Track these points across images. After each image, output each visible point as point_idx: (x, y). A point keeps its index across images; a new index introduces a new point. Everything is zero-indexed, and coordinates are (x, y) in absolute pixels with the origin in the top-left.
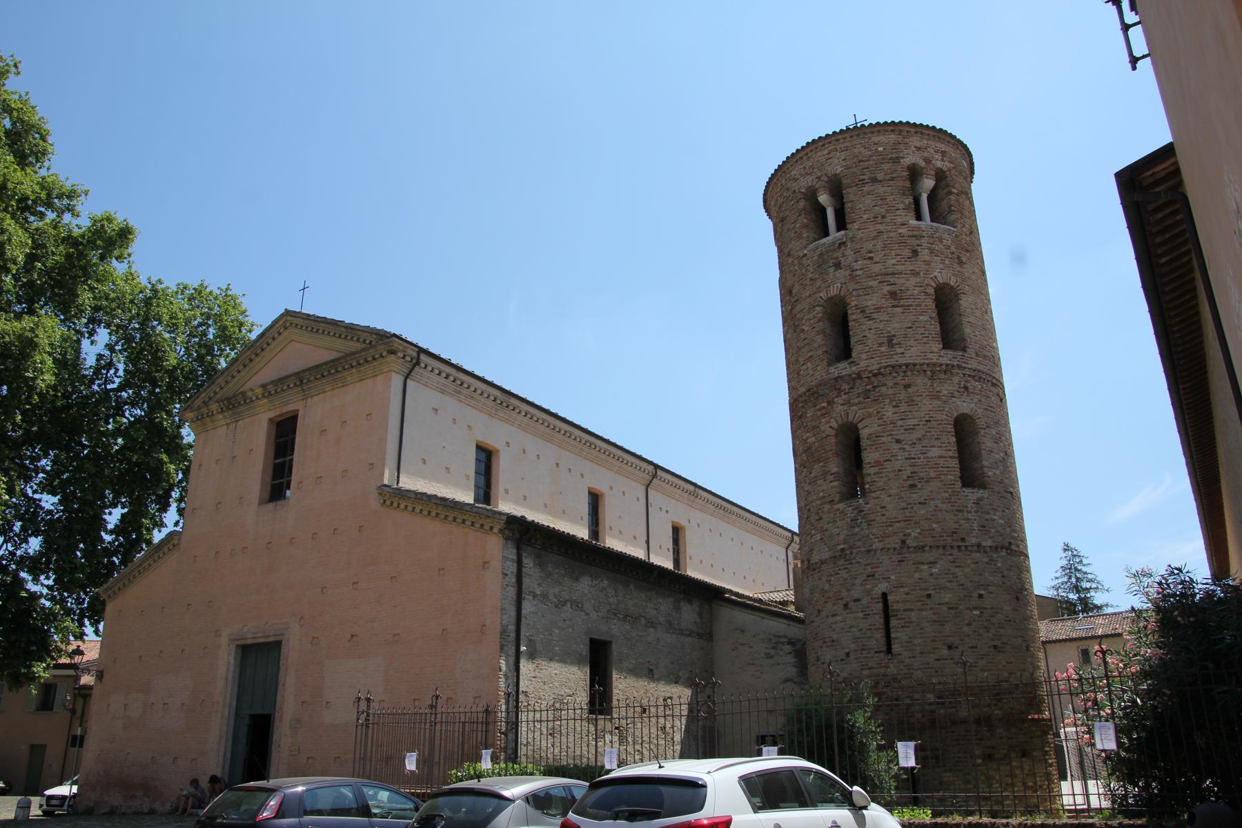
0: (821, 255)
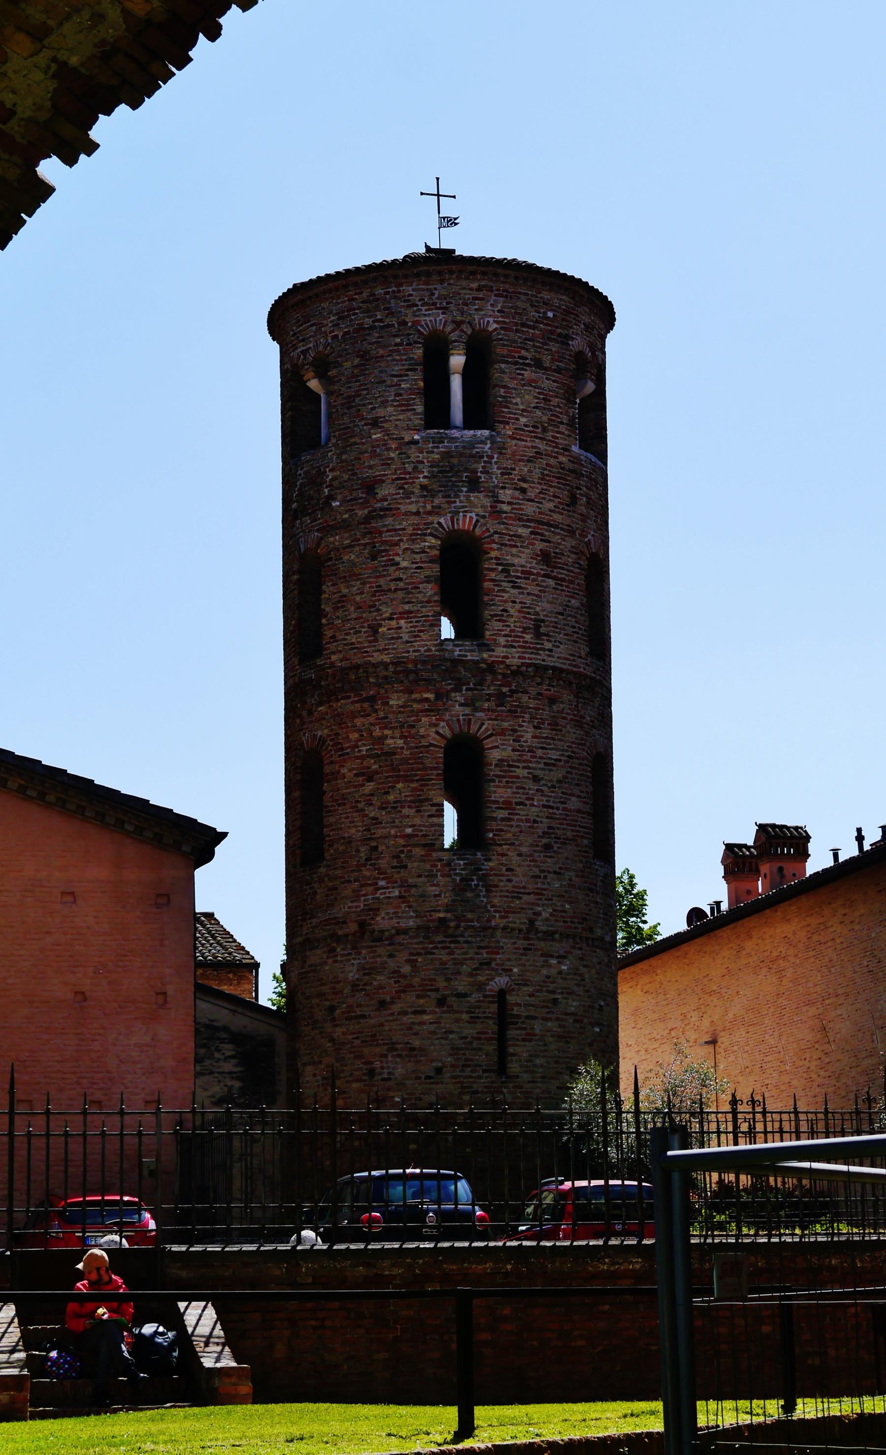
0: (447, 455)
